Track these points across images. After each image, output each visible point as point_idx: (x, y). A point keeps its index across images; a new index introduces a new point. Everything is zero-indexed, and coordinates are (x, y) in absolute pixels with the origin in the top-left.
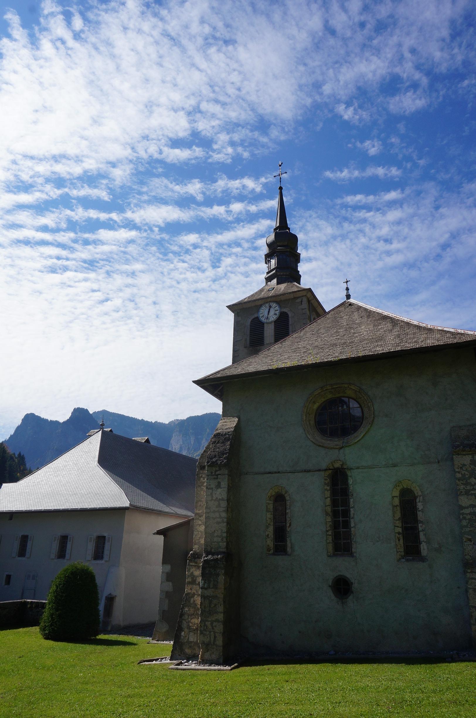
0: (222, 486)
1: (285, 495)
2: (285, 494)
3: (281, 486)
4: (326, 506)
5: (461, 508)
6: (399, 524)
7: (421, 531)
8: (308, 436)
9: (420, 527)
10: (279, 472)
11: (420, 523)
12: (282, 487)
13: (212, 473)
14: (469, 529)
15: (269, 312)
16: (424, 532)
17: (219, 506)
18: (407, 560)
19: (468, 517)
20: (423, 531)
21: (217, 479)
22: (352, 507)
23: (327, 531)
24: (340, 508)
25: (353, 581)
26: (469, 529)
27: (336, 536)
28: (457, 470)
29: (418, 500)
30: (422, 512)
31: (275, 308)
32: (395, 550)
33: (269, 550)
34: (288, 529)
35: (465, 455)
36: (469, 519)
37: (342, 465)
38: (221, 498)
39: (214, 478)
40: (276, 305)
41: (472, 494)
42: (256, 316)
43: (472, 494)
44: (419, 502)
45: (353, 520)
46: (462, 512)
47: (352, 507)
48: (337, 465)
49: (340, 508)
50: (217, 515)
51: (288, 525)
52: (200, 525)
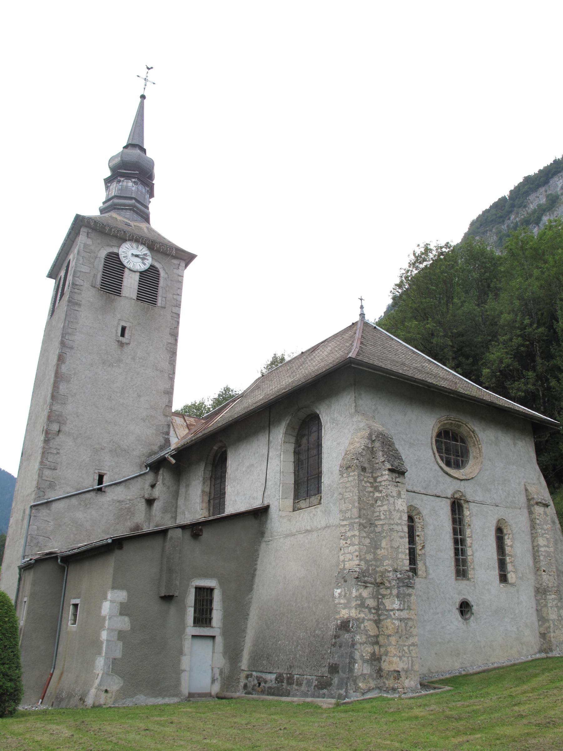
1: (415, 517)
2: (415, 515)
3: (416, 506)
7: (509, 563)
10: (414, 492)
11: (508, 556)
12: (416, 507)
16: (513, 564)
17: (400, 518)
19: (544, 554)
20: (511, 562)
21: (397, 486)
22: (469, 537)
25: (473, 603)
29: (506, 537)
30: (511, 547)
34: (419, 552)
36: (544, 556)
37: (461, 496)
44: (508, 539)
45: (471, 549)
47: (469, 537)
51: (419, 547)
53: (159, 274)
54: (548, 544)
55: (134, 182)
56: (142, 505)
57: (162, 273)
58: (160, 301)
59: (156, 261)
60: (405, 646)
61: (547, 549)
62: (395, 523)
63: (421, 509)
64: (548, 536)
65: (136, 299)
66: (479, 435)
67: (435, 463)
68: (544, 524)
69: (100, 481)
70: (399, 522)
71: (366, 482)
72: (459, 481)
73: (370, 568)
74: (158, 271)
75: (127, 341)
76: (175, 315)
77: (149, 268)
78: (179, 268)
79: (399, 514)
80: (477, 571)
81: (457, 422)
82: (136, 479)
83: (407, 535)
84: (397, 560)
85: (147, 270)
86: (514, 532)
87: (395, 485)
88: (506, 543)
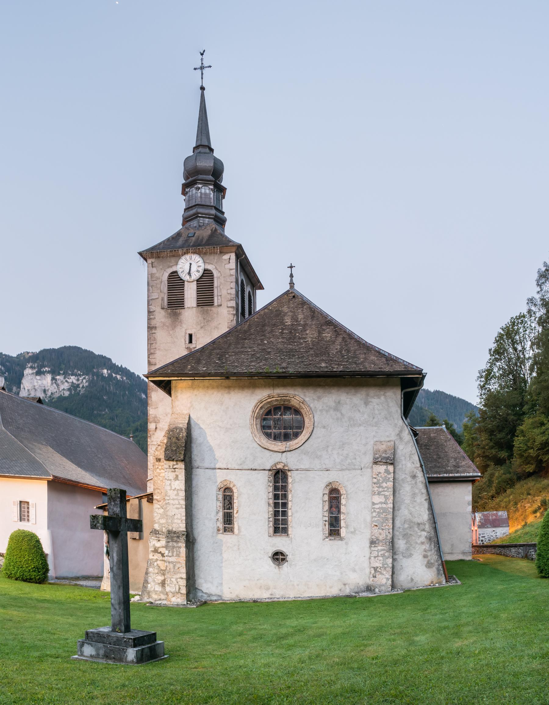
0: (179, 479)
1: (233, 488)
2: (233, 487)
4: (269, 499)
5: (374, 504)
6: (326, 514)
8: (255, 439)
9: (342, 517)
10: (228, 469)
12: (230, 481)
13: (170, 466)
14: (377, 519)
17: (177, 495)
18: (330, 540)
19: (378, 510)
20: (344, 519)
21: (175, 471)
22: (290, 501)
23: (269, 518)
24: (280, 501)
26: (377, 519)
27: (276, 522)
28: (374, 476)
29: (342, 497)
31: (197, 263)
32: (322, 532)
33: (218, 530)
34: (235, 515)
35: (381, 465)
36: (378, 512)
37: (284, 466)
38: (179, 488)
39: (172, 471)
40: (199, 259)
41: (382, 495)
42: (174, 269)
43: (382, 495)
46: (373, 507)
47: (290, 501)
48: (280, 466)
49: (280, 501)
50: (176, 502)
51: (235, 512)
52: (159, 508)
54: (386, 500)
59: (209, 263)
60: (173, 578)
61: (384, 506)
62: (171, 498)
63: (235, 482)
64: (387, 493)
66: (311, 405)
67: (254, 440)
68: (382, 482)
70: (175, 497)
71: (160, 470)
72: (280, 454)
73: (164, 529)
74: (212, 273)
77: (204, 273)
78: (229, 262)
79: (175, 492)
80: (295, 528)
81: (283, 398)
83: (184, 507)
84: (172, 524)
85: (202, 276)
86: (349, 492)
87: (172, 471)
88: (341, 502)
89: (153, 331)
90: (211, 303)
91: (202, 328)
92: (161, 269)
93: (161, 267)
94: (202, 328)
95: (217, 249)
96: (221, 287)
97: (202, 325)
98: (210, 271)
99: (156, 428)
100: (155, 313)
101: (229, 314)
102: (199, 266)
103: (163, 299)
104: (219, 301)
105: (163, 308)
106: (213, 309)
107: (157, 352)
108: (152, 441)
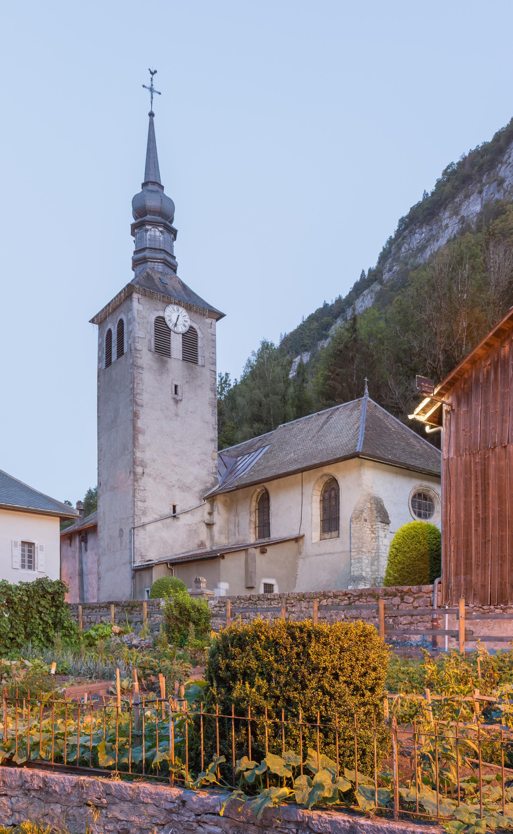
15: (178, 319)
17: (386, 550)
42: (161, 314)
53: (197, 335)
55: (161, 232)
56: (204, 529)
57: (200, 334)
58: (200, 361)
65: (181, 358)
69: (174, 511)
70: (385, 551)
71: (367, 528)
74: (196, 332)
75: (180, 398)
76: (212, 373)
79: (385, 547)
82: (198, 509)
85: (188, 332)
89: (140, 371)
90: (195, 362)
91: (187, 382)
92: (148, 309)
93: (148, 307)
94: (187, 382)
95: (206, 312)
96: (204, 348)
97: (188, 380)
98: (194, 329)
99: (143, 473)
100: (141, 352)
101: (211, 377)
102: (185, 321)
103: (150, 341)
104: (203, 362)
105: (150, 351)
106: (197, 367)
107: (144, 393)
108: (139, 486)
